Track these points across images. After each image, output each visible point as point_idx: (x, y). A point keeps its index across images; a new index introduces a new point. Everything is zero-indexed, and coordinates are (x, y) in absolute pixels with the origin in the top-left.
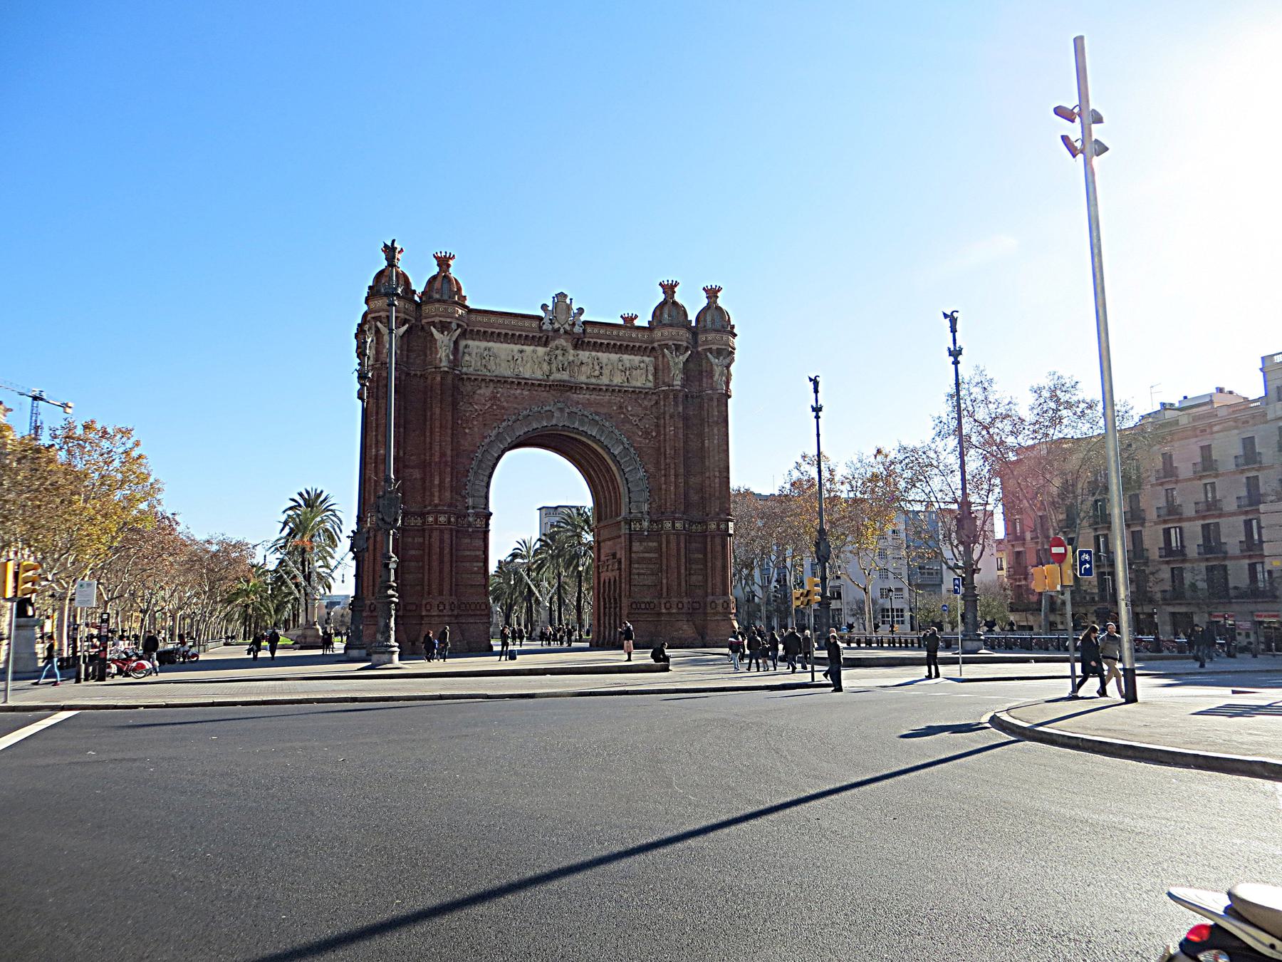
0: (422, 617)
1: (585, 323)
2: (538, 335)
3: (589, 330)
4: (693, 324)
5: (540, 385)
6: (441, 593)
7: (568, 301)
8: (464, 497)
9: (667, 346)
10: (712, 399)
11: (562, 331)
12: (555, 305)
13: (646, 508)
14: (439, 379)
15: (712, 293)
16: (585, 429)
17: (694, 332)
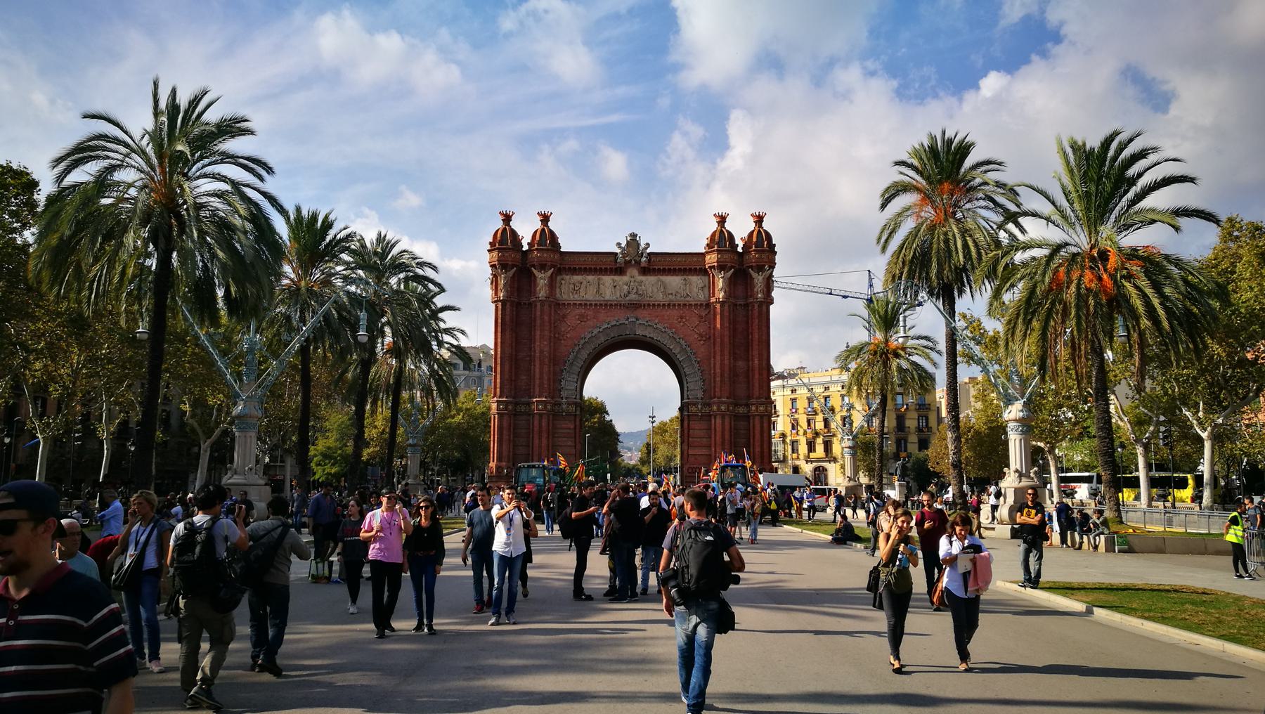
1: (650, 254)
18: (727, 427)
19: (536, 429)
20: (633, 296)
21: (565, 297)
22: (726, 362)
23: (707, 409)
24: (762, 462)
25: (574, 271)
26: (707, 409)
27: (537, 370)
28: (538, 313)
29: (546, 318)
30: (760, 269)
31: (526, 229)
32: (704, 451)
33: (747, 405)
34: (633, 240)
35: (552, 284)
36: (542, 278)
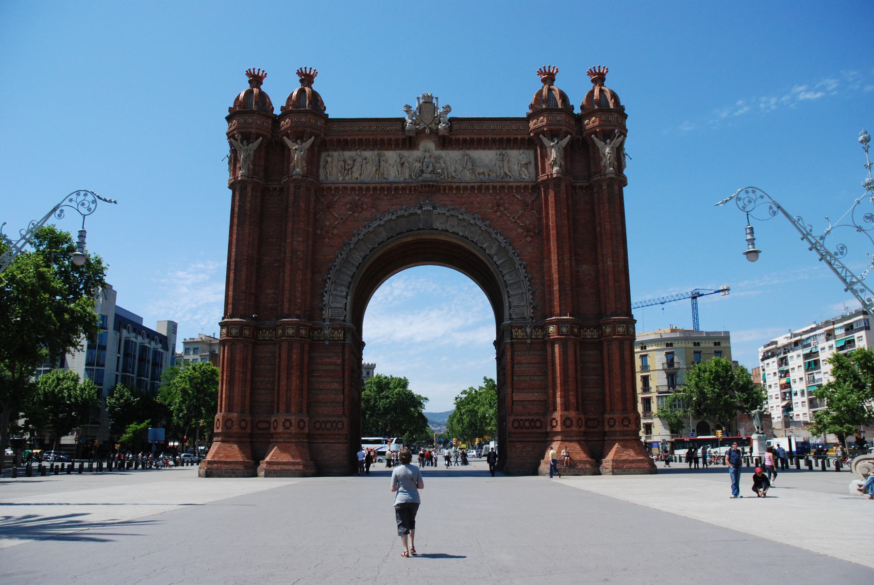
0: (272, 435)
1: (451, 120)
2: (401, 137)
3: (456, 126)
4: (577, 111)
5: (404, 188)
6: (288, 411)
7: (434, 101)
8: (322, 309)
9: (543, 133)
10: (601, 186)
11: (427, 131)
12: (420, 108)
13: (528, 312)
14: (292, 185)
15: (599, 78)
16: (455, 230)
17: (579, 119)
18: (571, 359)
19: (284, 363)
20: (427, 176)
21: (332, 178)
22: (567, 263)
23: (540, 334)
24: (624, 410)
25: (345, 145)
26: (540, 334)
27: (287, 278)
28: (291, 198)
29: (302, 205)
30: (607, 136)
31: (280, 92)
32: (536, 396)
33: (598, 327)
34: (428, 102)
35: (313, 159)
36: (298, 152)
